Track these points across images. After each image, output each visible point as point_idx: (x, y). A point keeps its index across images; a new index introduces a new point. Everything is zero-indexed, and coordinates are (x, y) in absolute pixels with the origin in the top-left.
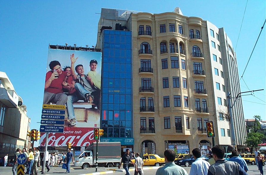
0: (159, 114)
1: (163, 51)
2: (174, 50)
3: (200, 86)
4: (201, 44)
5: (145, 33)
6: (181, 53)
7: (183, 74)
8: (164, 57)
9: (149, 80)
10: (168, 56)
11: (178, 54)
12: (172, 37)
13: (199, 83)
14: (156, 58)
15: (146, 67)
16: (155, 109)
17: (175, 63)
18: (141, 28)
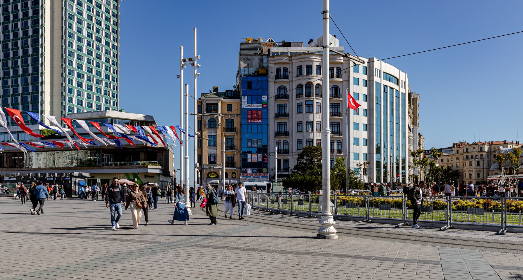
0: (293, 155)
1: (299, 95)
2: (309, 95)
3: (336, 128)
4: (341, 83)
5: (282, 77)
6: (317, 95)
7: (317, 118)
8: (299, 101)
9: (285, 124)
10: (303, 100)
11: (313, 97)
12: (308, 81)
13: (335, 125)
14: (292, 104)
15: (282, 113)
16: (290, 151)
17: (310, 106)
18: (278, 70)
